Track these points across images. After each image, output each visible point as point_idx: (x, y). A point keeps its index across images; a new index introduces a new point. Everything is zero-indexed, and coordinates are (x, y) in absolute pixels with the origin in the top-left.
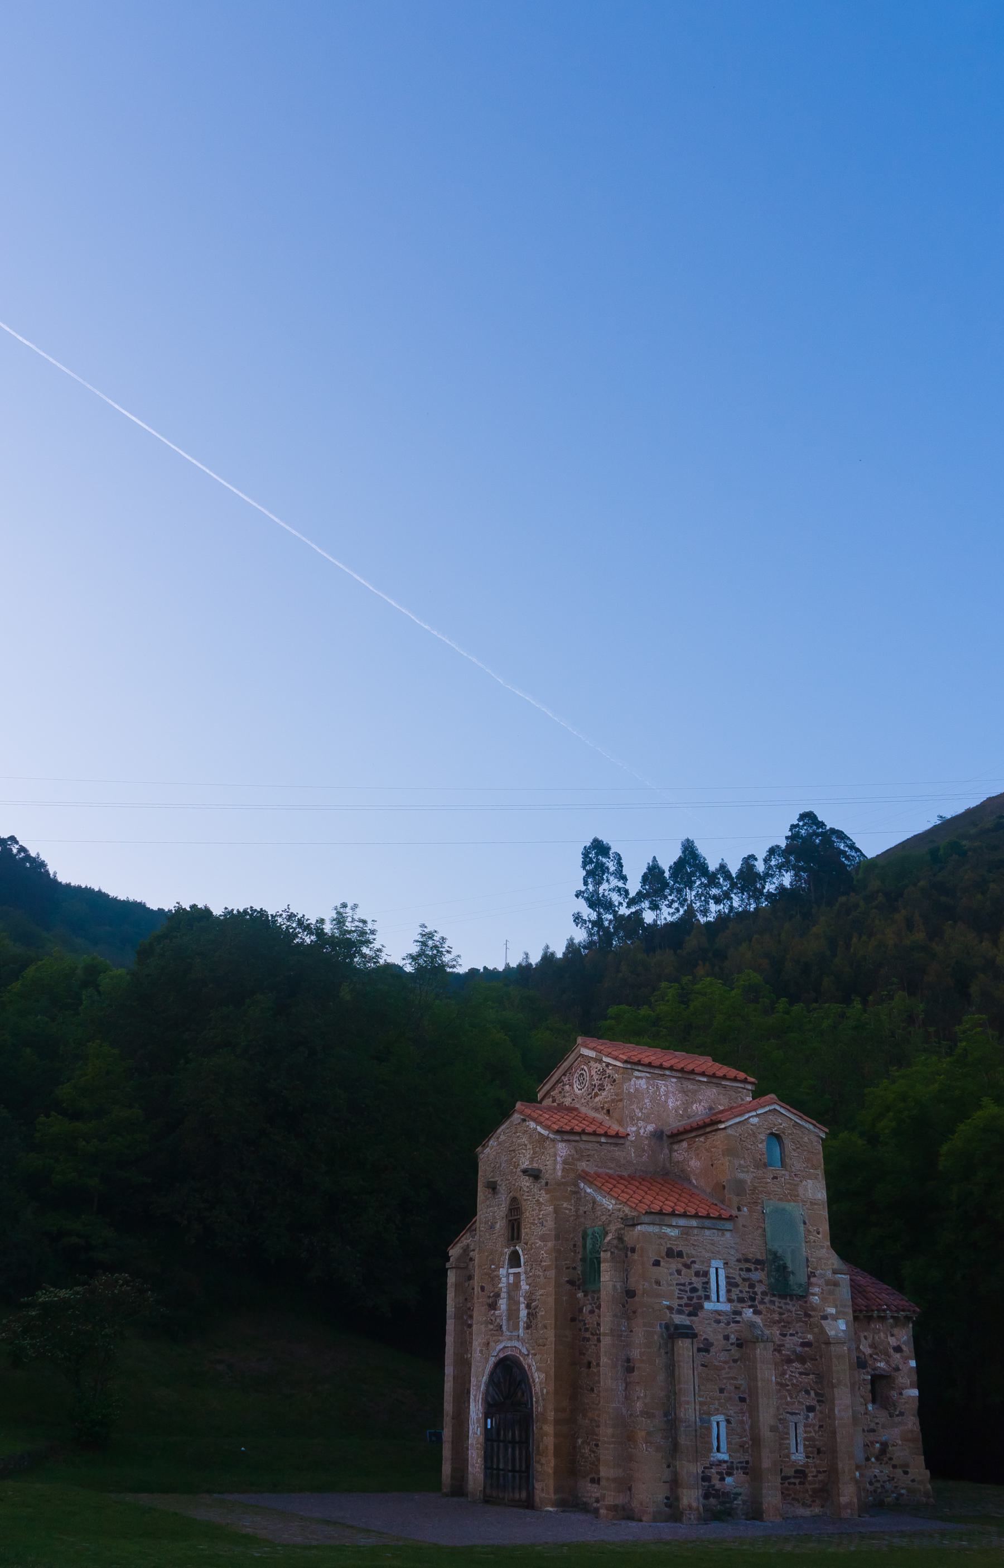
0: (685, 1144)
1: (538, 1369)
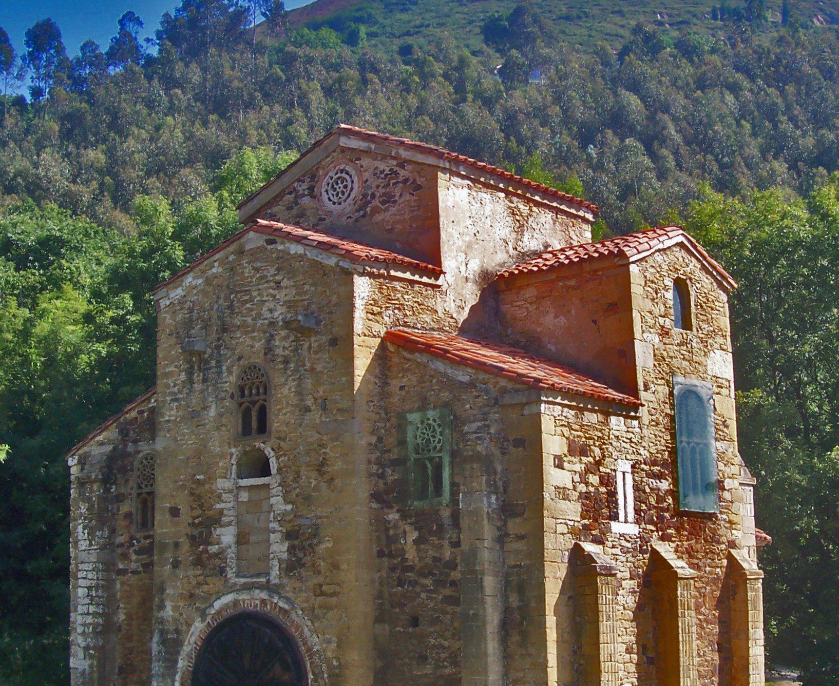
0: (530, 293)
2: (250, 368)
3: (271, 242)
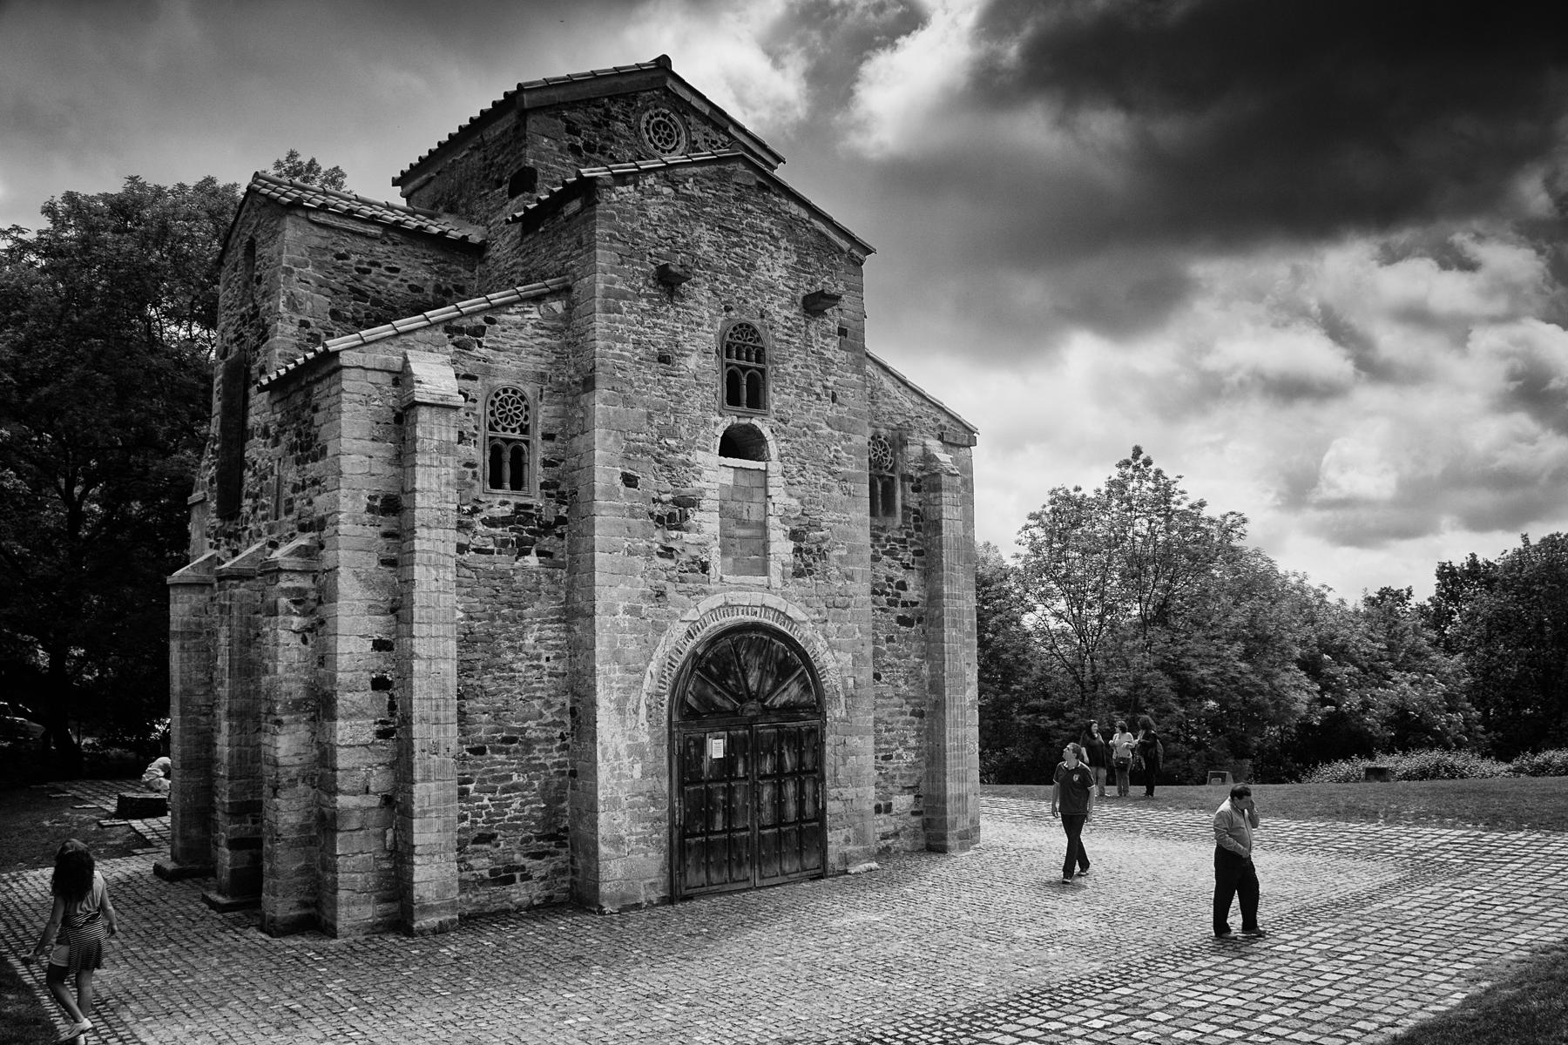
1: (832, 647)
2: (741, 326)
3: (761, 187)
